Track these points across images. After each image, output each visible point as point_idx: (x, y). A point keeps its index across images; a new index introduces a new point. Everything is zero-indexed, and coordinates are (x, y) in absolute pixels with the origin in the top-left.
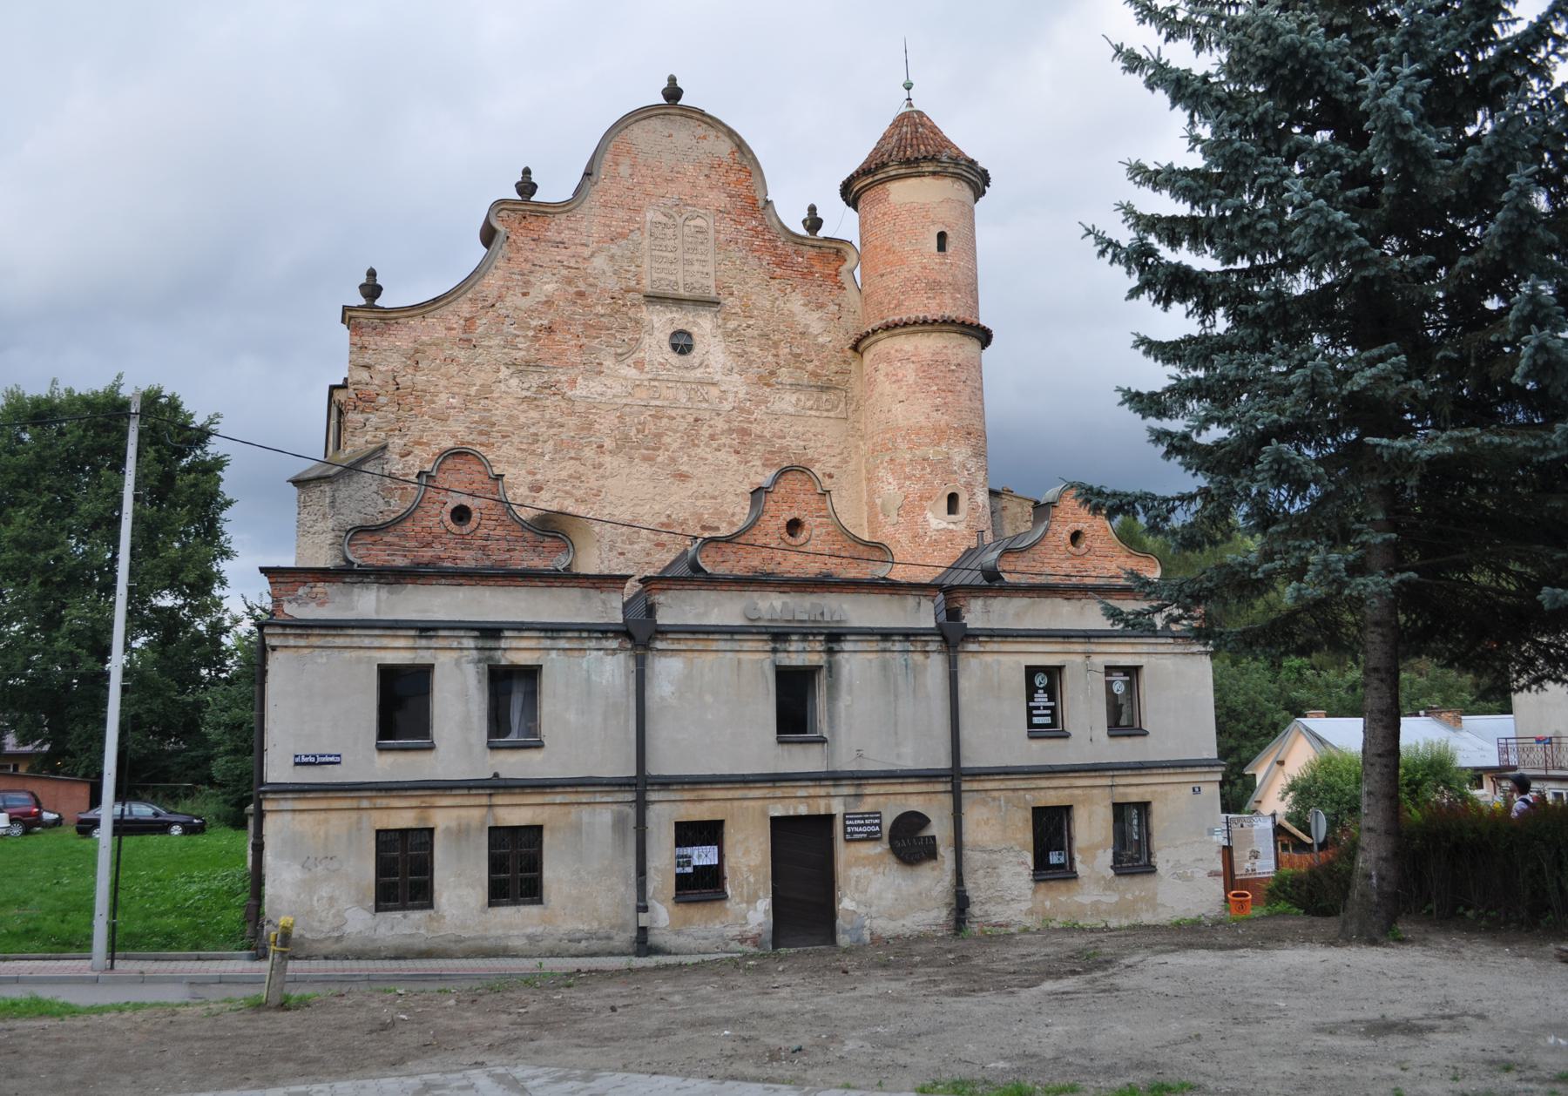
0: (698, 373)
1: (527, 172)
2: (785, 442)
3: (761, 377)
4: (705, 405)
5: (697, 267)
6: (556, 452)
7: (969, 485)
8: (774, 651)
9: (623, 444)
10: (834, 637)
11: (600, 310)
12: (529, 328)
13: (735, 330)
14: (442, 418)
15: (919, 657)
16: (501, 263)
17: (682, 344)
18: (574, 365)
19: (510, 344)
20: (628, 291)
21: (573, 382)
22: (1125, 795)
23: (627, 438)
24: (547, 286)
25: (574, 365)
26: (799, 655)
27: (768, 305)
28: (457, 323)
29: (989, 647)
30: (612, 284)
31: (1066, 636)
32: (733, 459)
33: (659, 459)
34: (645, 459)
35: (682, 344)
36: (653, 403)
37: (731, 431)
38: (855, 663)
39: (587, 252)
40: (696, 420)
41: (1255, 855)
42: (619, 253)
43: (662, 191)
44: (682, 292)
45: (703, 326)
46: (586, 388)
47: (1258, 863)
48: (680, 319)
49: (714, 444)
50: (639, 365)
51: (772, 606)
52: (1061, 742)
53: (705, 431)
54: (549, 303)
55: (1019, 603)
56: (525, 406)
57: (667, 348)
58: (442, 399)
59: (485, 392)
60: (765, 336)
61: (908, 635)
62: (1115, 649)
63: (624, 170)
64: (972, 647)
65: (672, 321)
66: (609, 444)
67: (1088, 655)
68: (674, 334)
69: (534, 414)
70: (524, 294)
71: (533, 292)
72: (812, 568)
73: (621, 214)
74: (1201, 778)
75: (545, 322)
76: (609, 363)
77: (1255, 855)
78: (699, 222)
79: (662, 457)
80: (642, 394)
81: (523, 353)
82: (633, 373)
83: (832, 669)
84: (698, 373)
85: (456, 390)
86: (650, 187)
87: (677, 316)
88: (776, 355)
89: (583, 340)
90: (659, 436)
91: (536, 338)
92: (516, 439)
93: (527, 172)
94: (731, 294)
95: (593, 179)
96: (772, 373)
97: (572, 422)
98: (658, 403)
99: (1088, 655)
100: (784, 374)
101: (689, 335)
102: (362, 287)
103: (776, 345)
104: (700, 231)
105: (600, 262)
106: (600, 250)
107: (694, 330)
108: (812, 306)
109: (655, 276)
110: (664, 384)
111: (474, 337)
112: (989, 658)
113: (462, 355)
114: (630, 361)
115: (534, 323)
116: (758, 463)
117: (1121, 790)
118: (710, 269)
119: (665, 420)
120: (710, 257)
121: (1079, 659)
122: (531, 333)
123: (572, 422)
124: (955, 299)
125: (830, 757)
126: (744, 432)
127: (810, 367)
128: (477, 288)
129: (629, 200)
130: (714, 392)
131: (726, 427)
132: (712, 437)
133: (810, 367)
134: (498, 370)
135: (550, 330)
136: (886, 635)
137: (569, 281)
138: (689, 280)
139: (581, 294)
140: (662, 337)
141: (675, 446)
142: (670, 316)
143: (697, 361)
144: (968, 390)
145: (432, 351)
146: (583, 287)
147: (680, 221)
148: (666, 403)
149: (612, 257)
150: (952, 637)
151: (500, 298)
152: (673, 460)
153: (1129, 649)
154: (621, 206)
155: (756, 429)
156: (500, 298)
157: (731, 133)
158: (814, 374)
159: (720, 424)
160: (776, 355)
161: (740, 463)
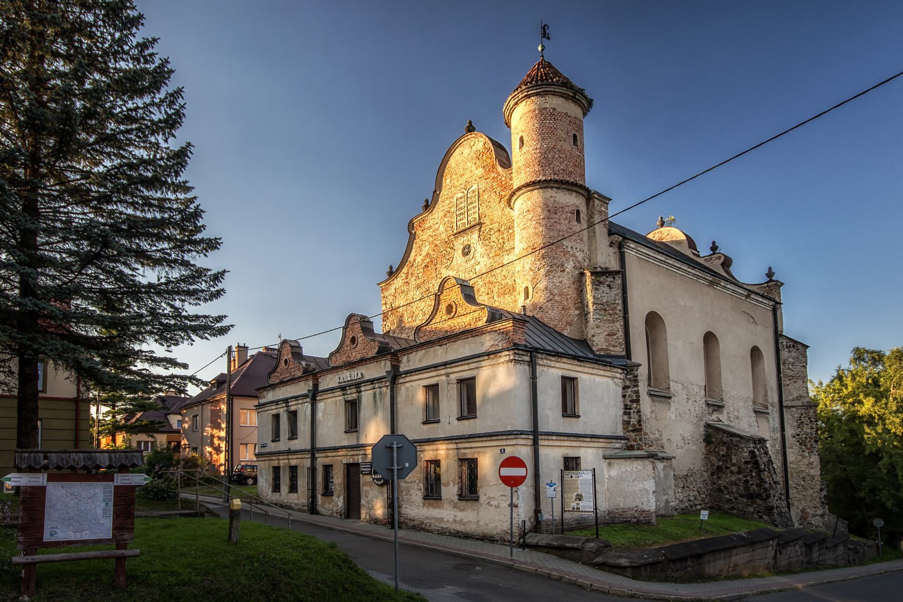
8: (344, 395)
10: (358, 385)
15: (384, 389)
22: (464, 454)
26: (352, 395)
29: (408, 379)
31: (435, 367)
38: (367, 396)
41: (579, 498)
44: (467, 226)
47: (581, 503)
51: (347, 376)
52: (436, 425)
55: (421, 353)
61: (379, 379)
62: (459, 369)
63: (448, 181)
64: (401, 381)
67: (447, 375)
72: (359, 357)
73: (448, 202)
74: (504, 443)
77: (579, 498)
83: (359, 398)
84: (472, 262)
88: (503, 238)
96: (500, 249)
99: (447, 375)
112: (408, 385)
117: (463, 451)
121: (444, 378)
125: (358, 438)
136: (372, 381)
150: (395, 376)
153: (466, 367)
160: (503, 238)
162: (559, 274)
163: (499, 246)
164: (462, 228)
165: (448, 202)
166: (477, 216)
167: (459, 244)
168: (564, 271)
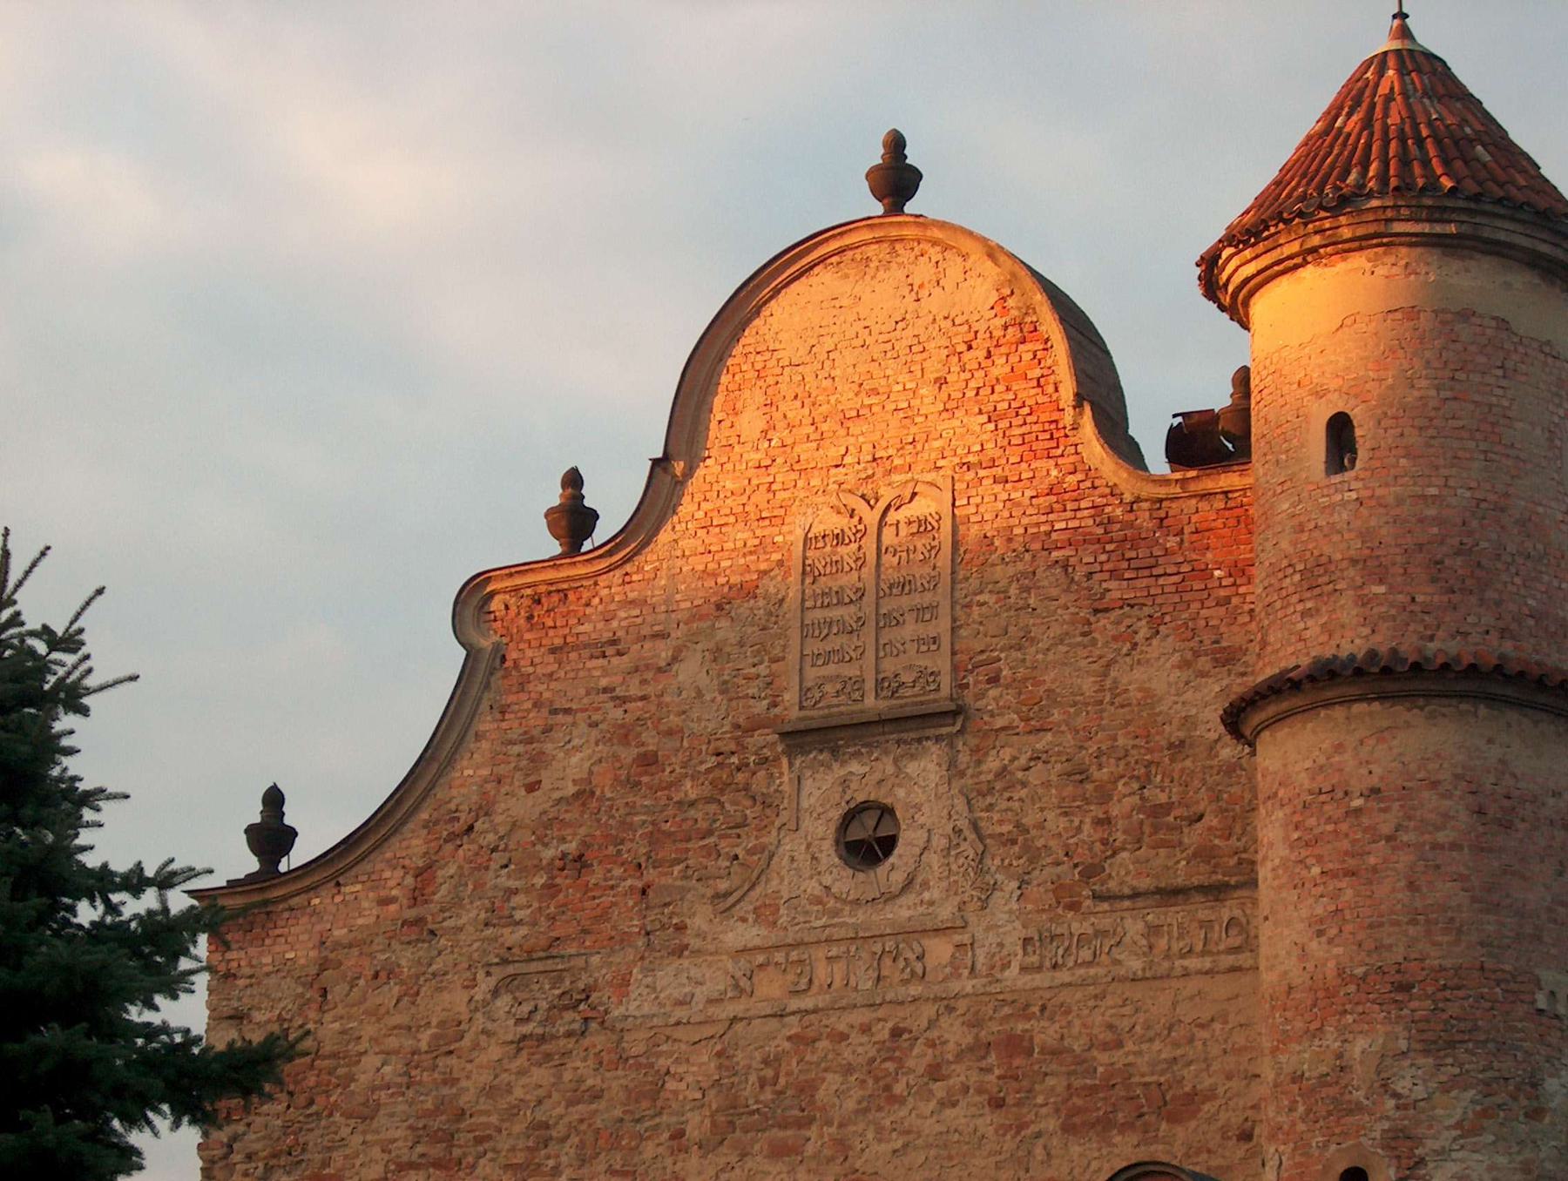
0: (903, 911)
1: (573, 480)
2: (1118, 1057)
3: (1059, 888)
4: (915, 990)
5: (910, 629)
6: (583, 1162)
7: (1400, 1141)
9: (732, 1122)
11: (690, 790)
12: (538, 867)
13: (1002, 772)
14: (366, 1114)
16: (486, 724)
17: (867, 841)
18: (625, 939)
19: (497, 916)
20: (751, 730)
21: (623, 983)
23: (733, 1106)
24: (574, 761)
25: (625, 939)
27: (1088, 685)
28: (396, 882)
30: (711, 719)
32: (987, 1122)
33: (810, 1149)
34: (778, 1152)
35: (867, 841)
36: (794, 1004)
37: (980, 1049)
39: (664, 652)
40: (896, 1033)
42: (733, 638)
43: (834, 453)
44: (872, 703)
45: (919, 785)
46: (653, 994)
48: (860, 775)
49: (939, 1089)
50: (765, 914)
53: (919, 1057)
54: (584, 794)
56: (521, 1061)
57: (829, 855)
58: (368, 1070)
59: (449, 1038)
60: (1079, 774)
63: (751, 423)
65: (844, 783)
66: (696, 1125)
68: (849, 818)
69: (542, 1075)
70: (532, 788)
71: (547, 779)
75: (572, 847)
76: (700, 920)
78: (922, 507)
79: (816, 1139)
80: (771, 987)
81: (523, 931)
82: (751, 934)
84: (903, 911)
85: (392, 1042)
86: (805, 451)
87: (855, 767)
88: (1105, 822)
89: (651, 874)
90: (807, 1089)
91: (551, 889)
92: (504, 1144)
93: (573, 480)
94: (994, 680)
95: (679, 467)
96: (1091, 872)
97: (617, 1082)
98: (807, 1002)
100: (1124, 871)
101: (886, 811)
102: (251, 831)
103: (1104, 795)
104: (923, 526)
105: (691, 671)
106: (693, 638)
107: (899, 797)
108: (1204, 663)
109: (812, 673)
110: (820, 953)
111: (428, 911)
113: (405, 958)
114: (746, 907)
115: (548, 854)
116: (1052, 1124)
118: (943, 626)
119: (823, 1044)
120: (942, 597)
122: (540, 880)
123: (617, 1082)
124: (1364, 601)
126: (1015, 1045)
127: (1193, 837)
128: (440, 793)
129: (761, 497)
130: (940, 950)
131: (970, 1039)
132: (935, 1072)
133: (1193, 837)
134: (472, 984)
135: (580, 861)
137: (625, 734)
138: (889, 666)
139: (649, 761)
140: (821, 829)
141: (850, 1105)
142: (839, 771)
143: (898, 878)
144: (1404, 859)
145: (351, 960)
146: (651, 740)
147: (872, 518)
148: (822, 1001)
149: (717, 653)
151: (484, 809)
152: (842, 1145)
154: (743, 517)
155: (1045, 1033)
156: (484, 809)
157: (993, 252)
158: (1205, 854)
159: (955, 1033)
160: (1105, 822)
161: (1003, 1130)
162: (1522, 1129)
163: (1082, 855)
164: (842, 707)
165: (741, 535)
166: (943, 663)
167: (820, 792)
168: (1535, 1114)
